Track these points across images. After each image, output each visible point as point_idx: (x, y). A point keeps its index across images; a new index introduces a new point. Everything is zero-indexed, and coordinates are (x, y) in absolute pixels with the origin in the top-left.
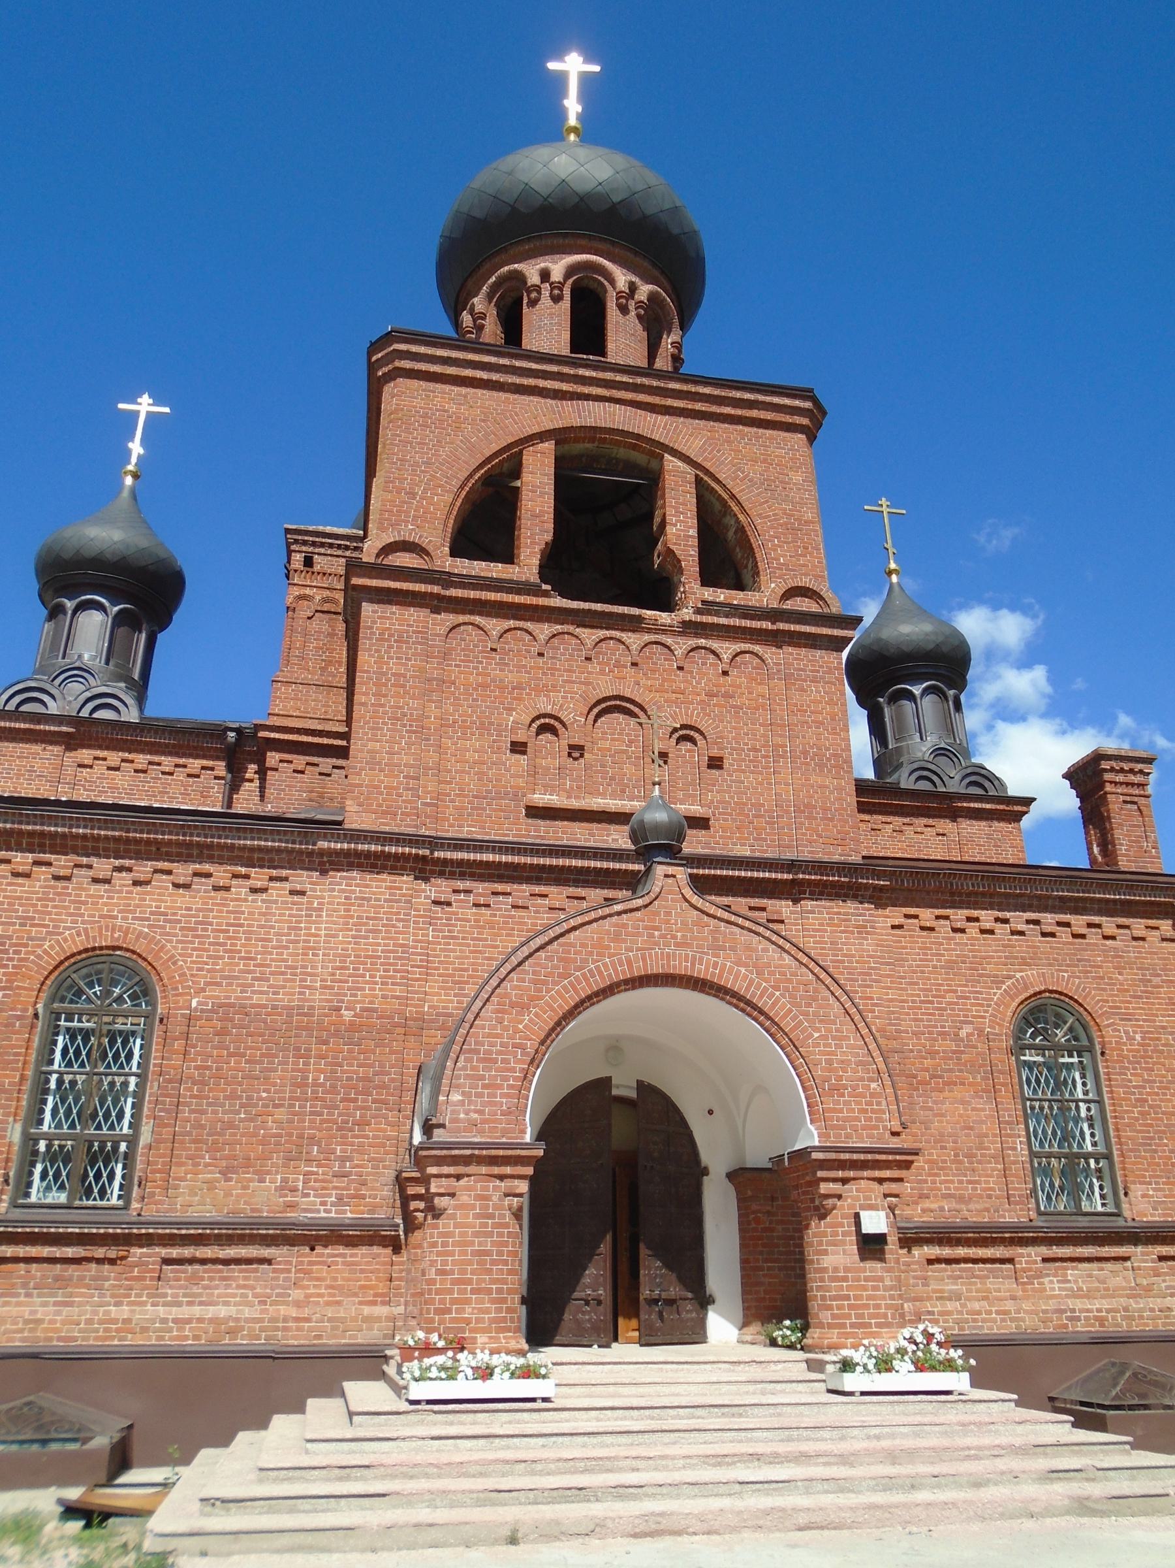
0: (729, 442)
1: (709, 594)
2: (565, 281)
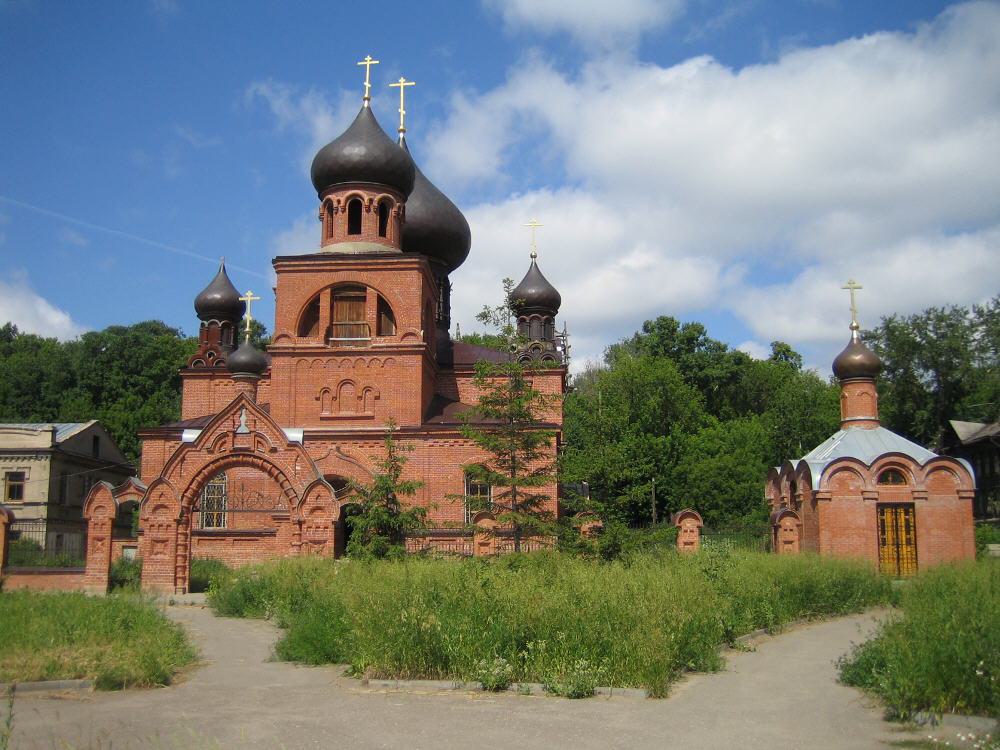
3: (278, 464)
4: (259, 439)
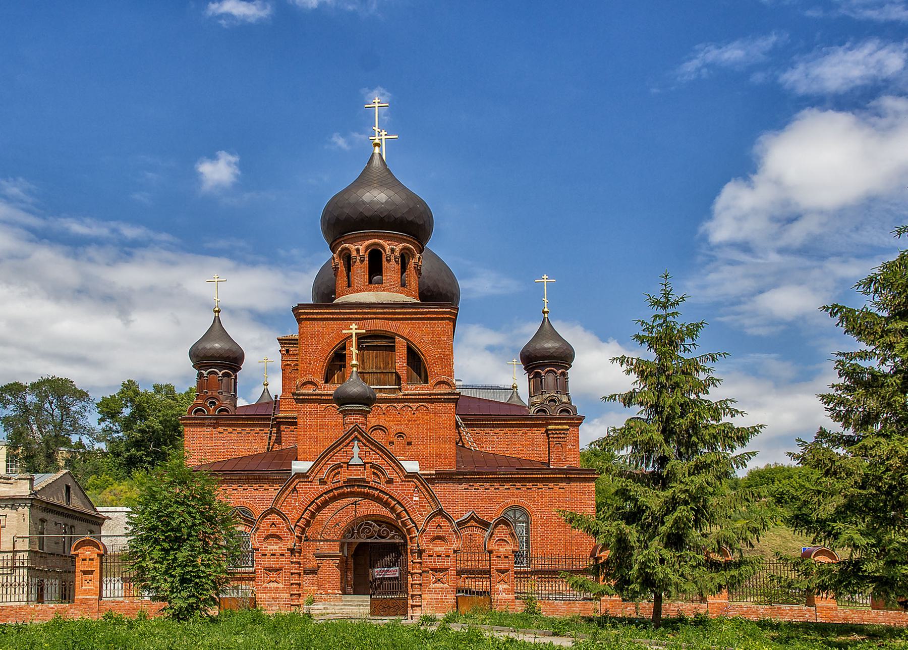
0: (419, 328)
1: (409, 387)
2: (365, 252)
3: (395, 495)
4: (376, 471)
